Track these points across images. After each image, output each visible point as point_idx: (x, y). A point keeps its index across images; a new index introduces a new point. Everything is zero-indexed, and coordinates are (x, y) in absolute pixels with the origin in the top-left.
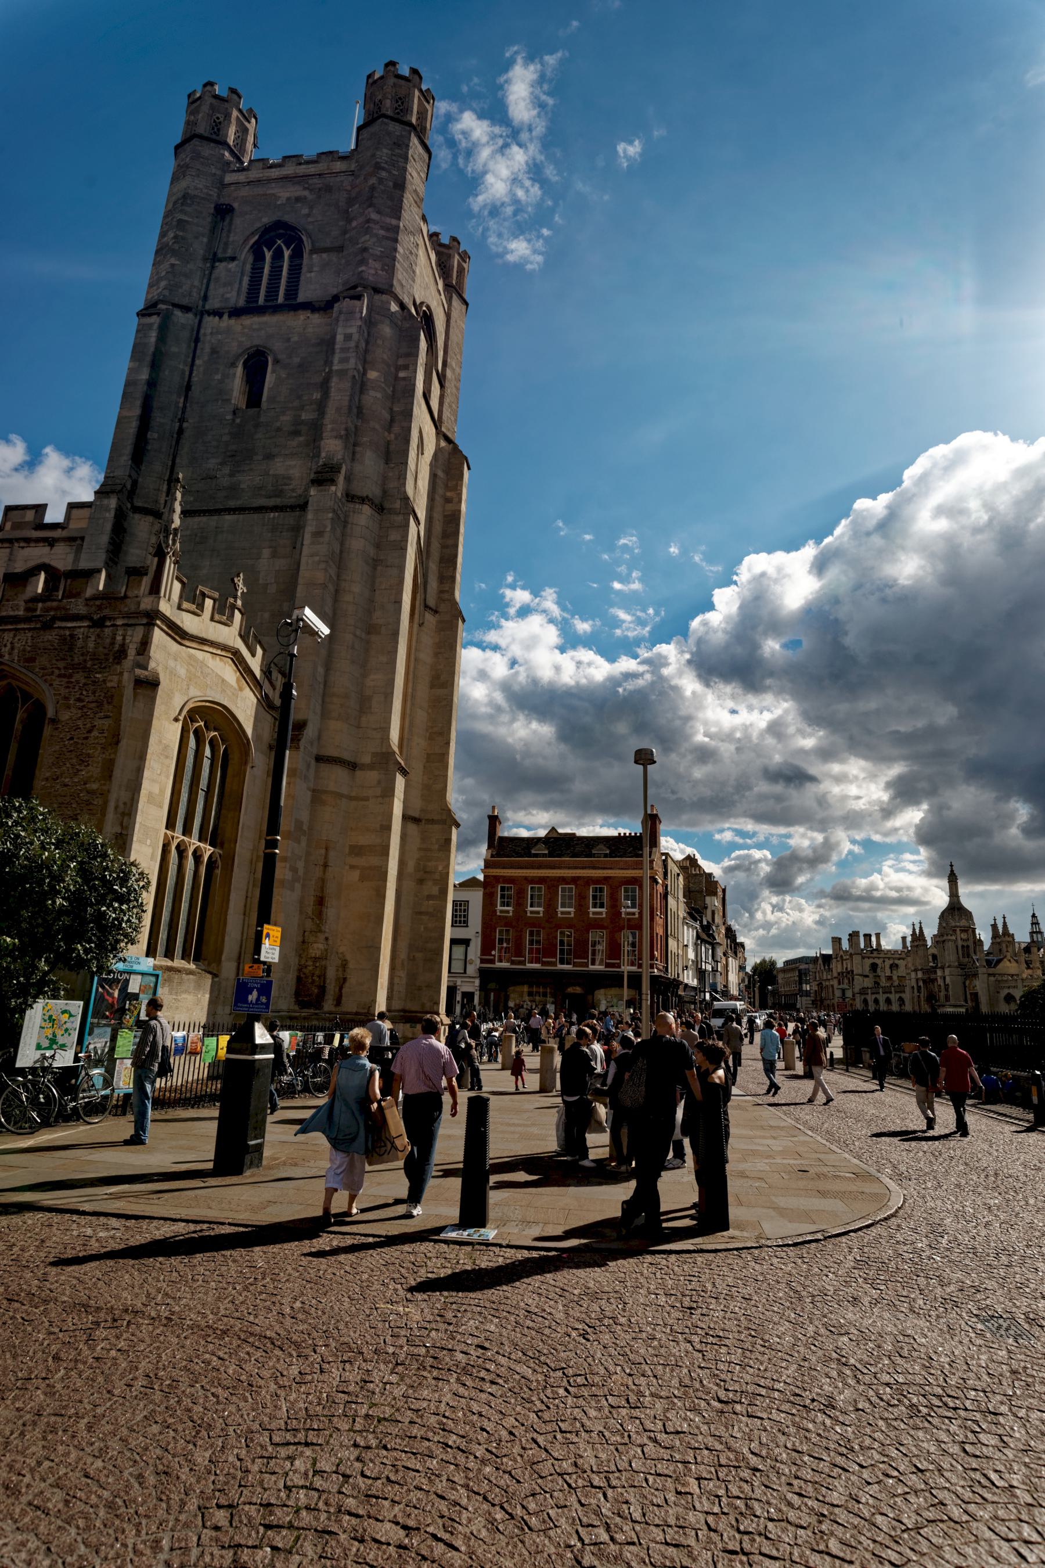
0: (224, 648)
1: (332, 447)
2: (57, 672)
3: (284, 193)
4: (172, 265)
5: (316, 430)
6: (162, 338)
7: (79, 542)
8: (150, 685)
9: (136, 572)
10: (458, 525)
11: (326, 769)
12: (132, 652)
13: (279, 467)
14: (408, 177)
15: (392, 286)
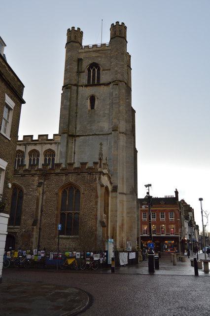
13: (101, 124)
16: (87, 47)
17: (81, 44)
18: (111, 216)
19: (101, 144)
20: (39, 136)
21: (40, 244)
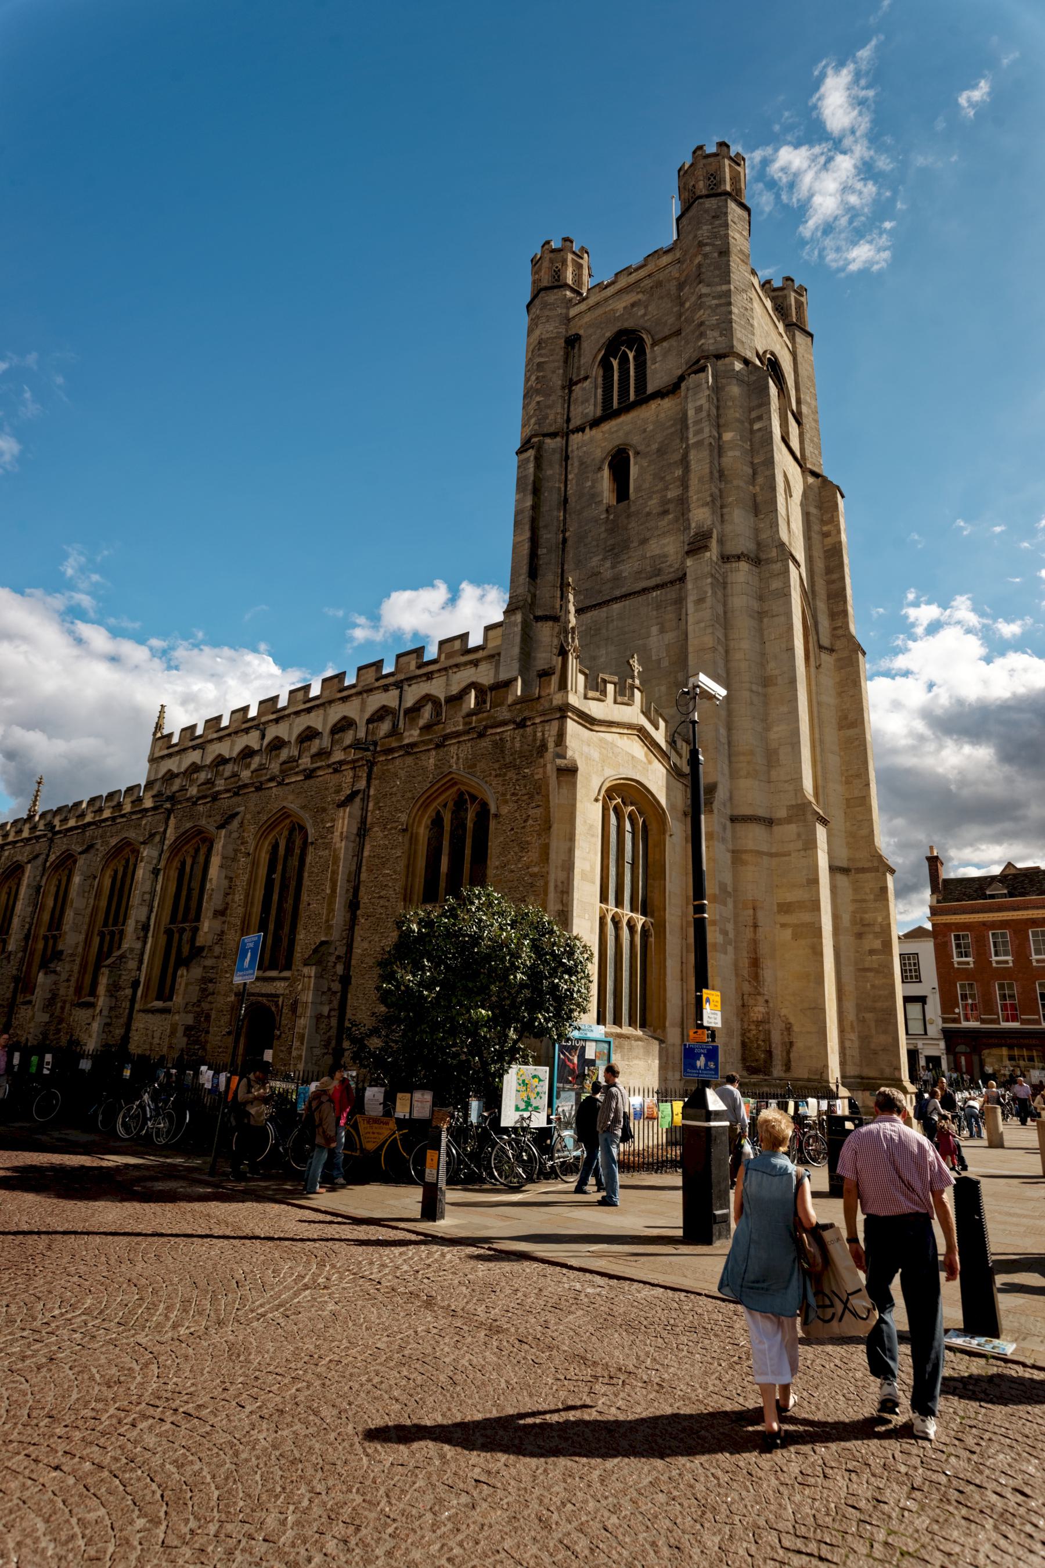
0: (630, 726)
2: (494, 773)
3: (620, 305)
4: (538, 402)
5: (683, 502)
6: (538, 466)
7: (497, 658)
8: (571, 771)
9: (545, 674)
10: (841, 556)
11: (742, 828)
12: (551, 745)
13: (654, 548)
14: (731, 241)
15: (732, 347)
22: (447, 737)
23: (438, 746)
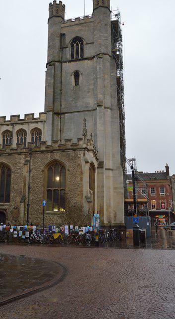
1: (100, 96)
16: (70, 20)
17: (63, 19)
18: (98, 192)
19: (85, 120)
20: (26, 115)
21: (29, 220)
22: (55, 150)
23: (52, 152)
